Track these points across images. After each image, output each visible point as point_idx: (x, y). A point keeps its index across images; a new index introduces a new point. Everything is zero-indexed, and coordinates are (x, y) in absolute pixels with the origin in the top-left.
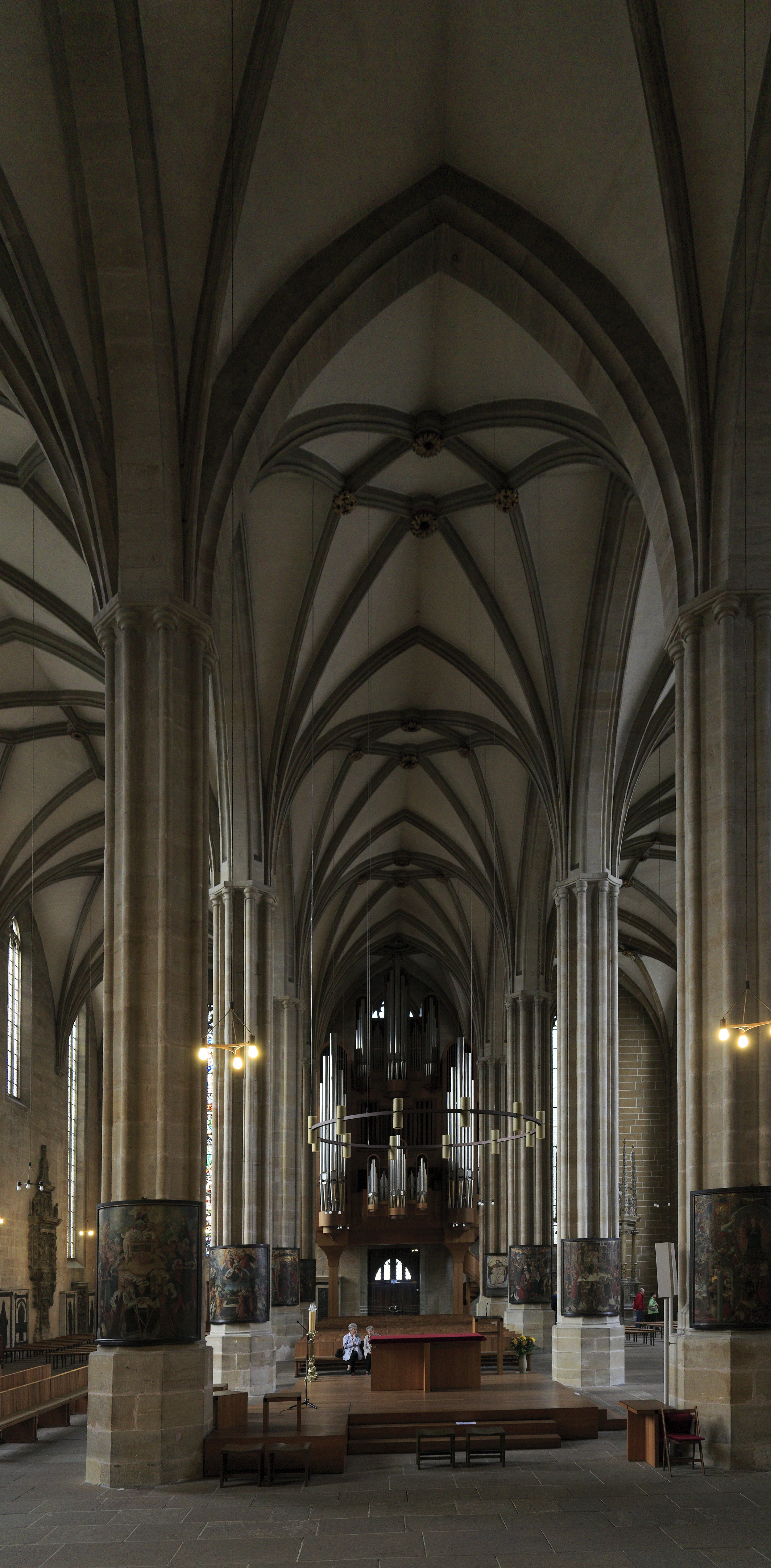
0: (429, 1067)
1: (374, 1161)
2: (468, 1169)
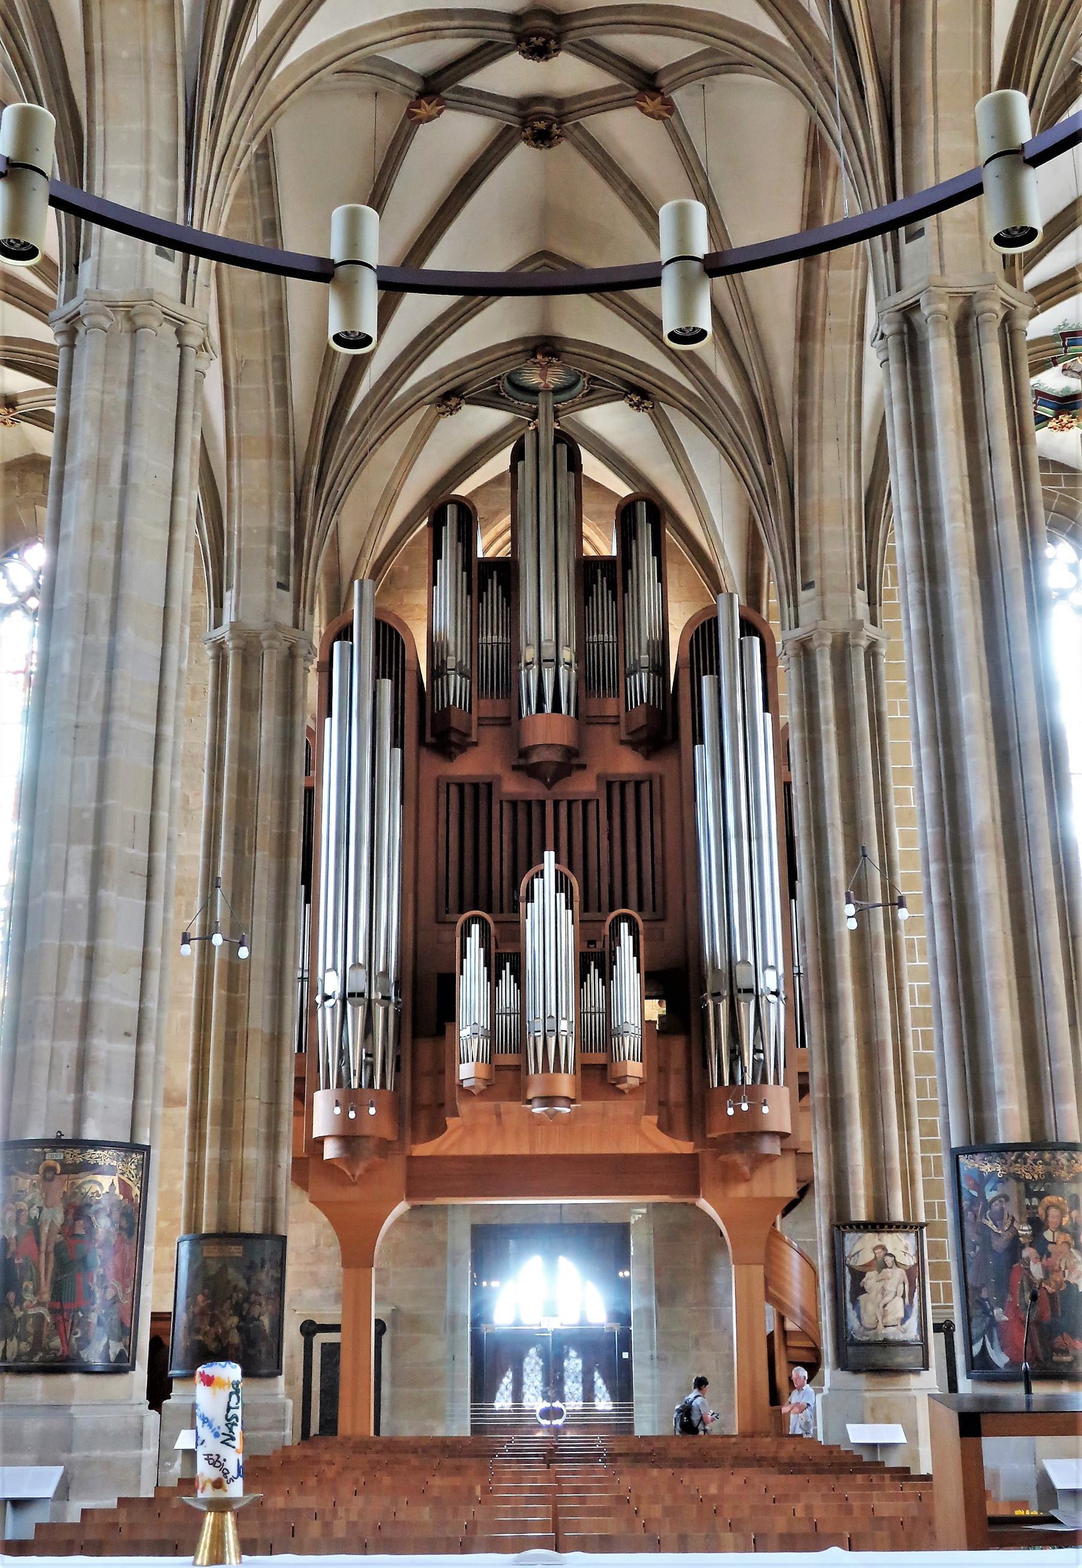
0: (642, 681)
1: (475, 929)
2: (766, 967)
